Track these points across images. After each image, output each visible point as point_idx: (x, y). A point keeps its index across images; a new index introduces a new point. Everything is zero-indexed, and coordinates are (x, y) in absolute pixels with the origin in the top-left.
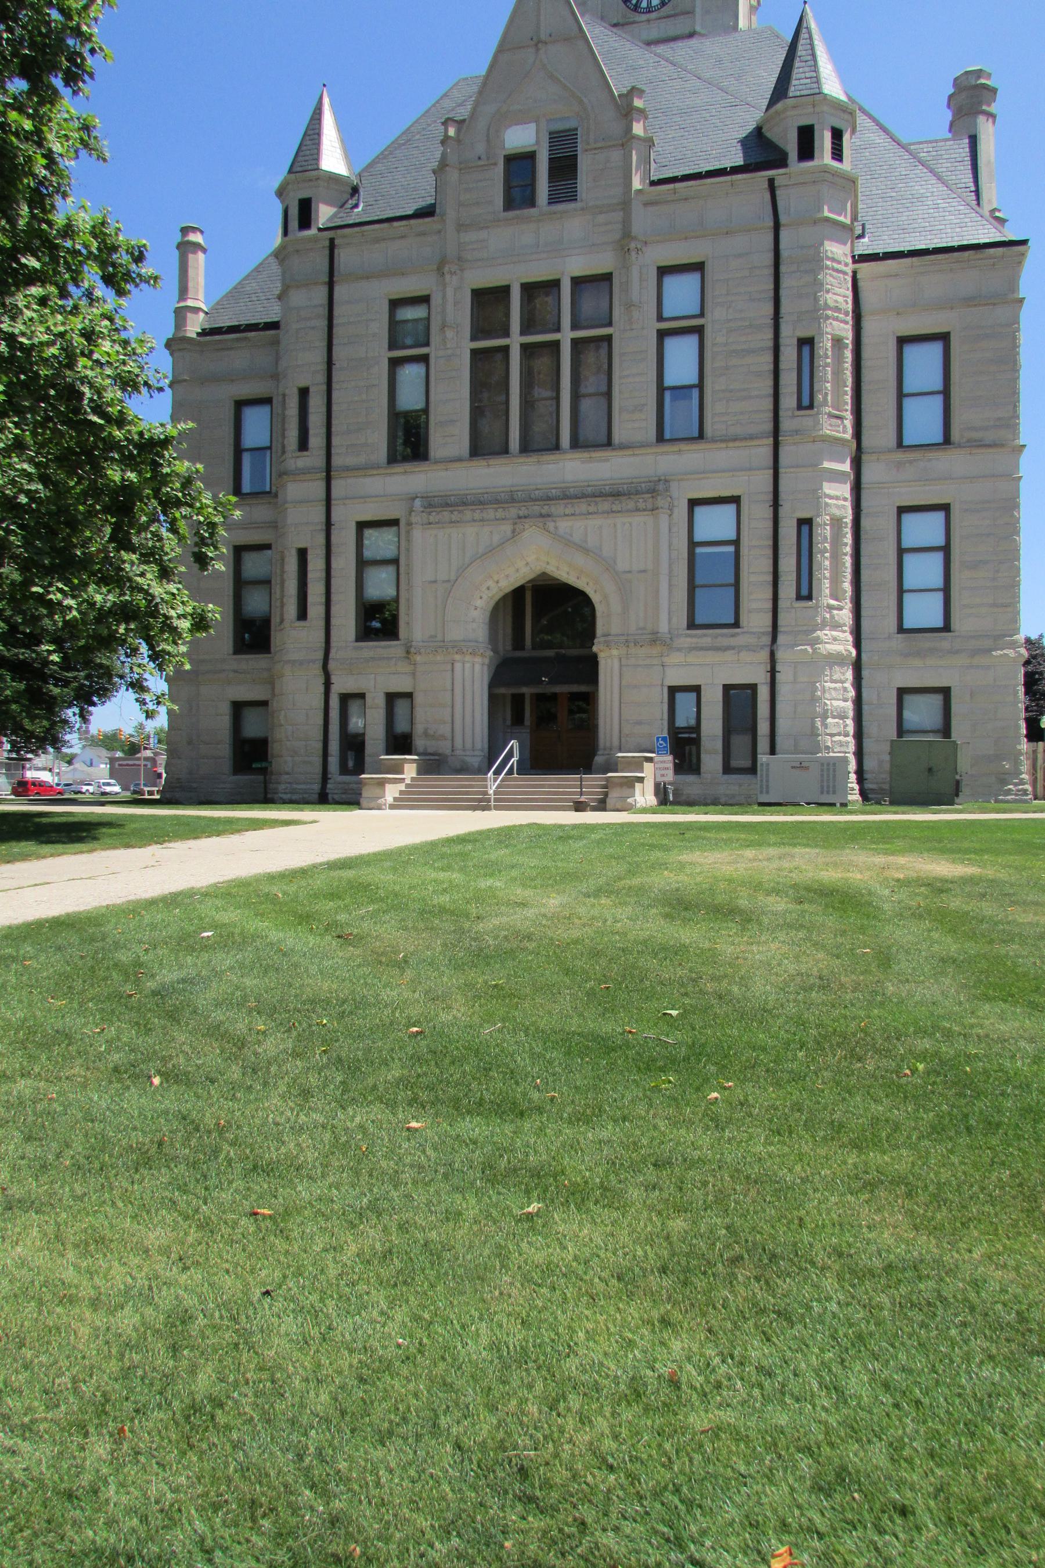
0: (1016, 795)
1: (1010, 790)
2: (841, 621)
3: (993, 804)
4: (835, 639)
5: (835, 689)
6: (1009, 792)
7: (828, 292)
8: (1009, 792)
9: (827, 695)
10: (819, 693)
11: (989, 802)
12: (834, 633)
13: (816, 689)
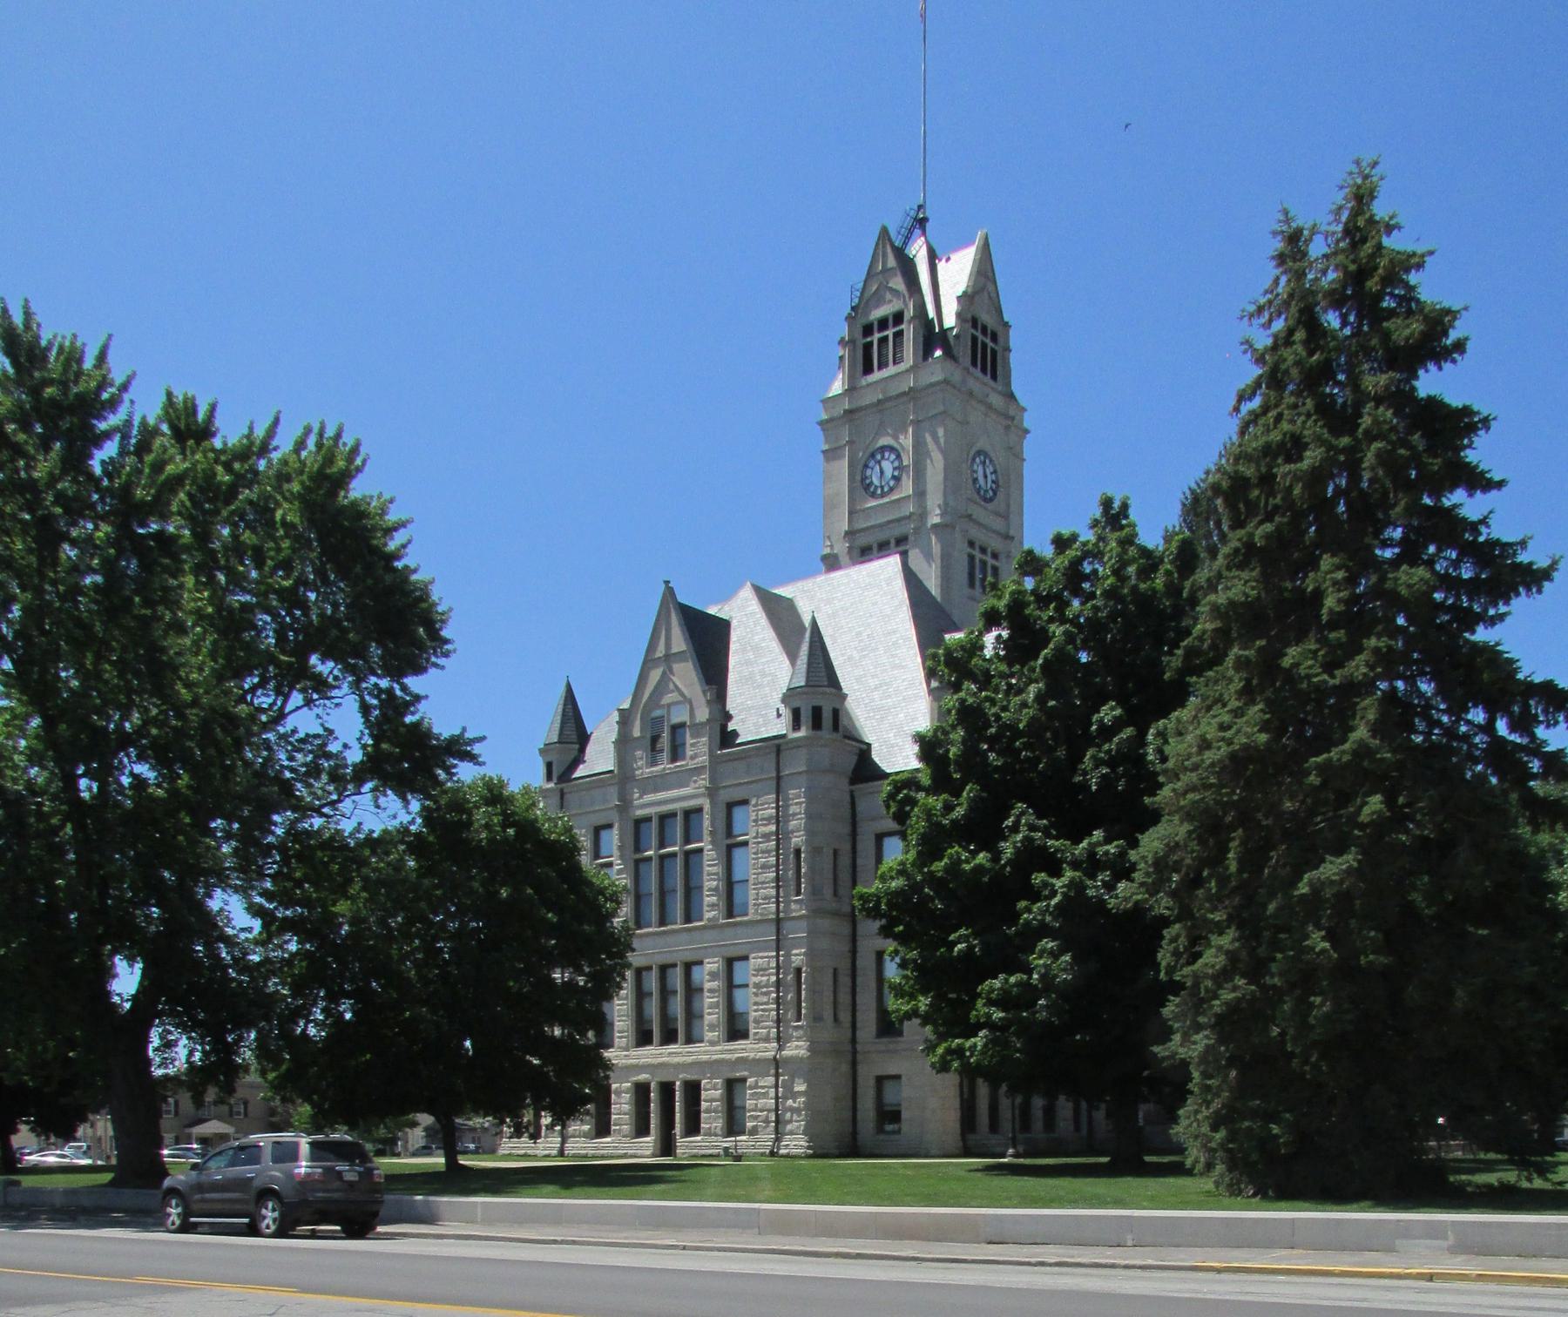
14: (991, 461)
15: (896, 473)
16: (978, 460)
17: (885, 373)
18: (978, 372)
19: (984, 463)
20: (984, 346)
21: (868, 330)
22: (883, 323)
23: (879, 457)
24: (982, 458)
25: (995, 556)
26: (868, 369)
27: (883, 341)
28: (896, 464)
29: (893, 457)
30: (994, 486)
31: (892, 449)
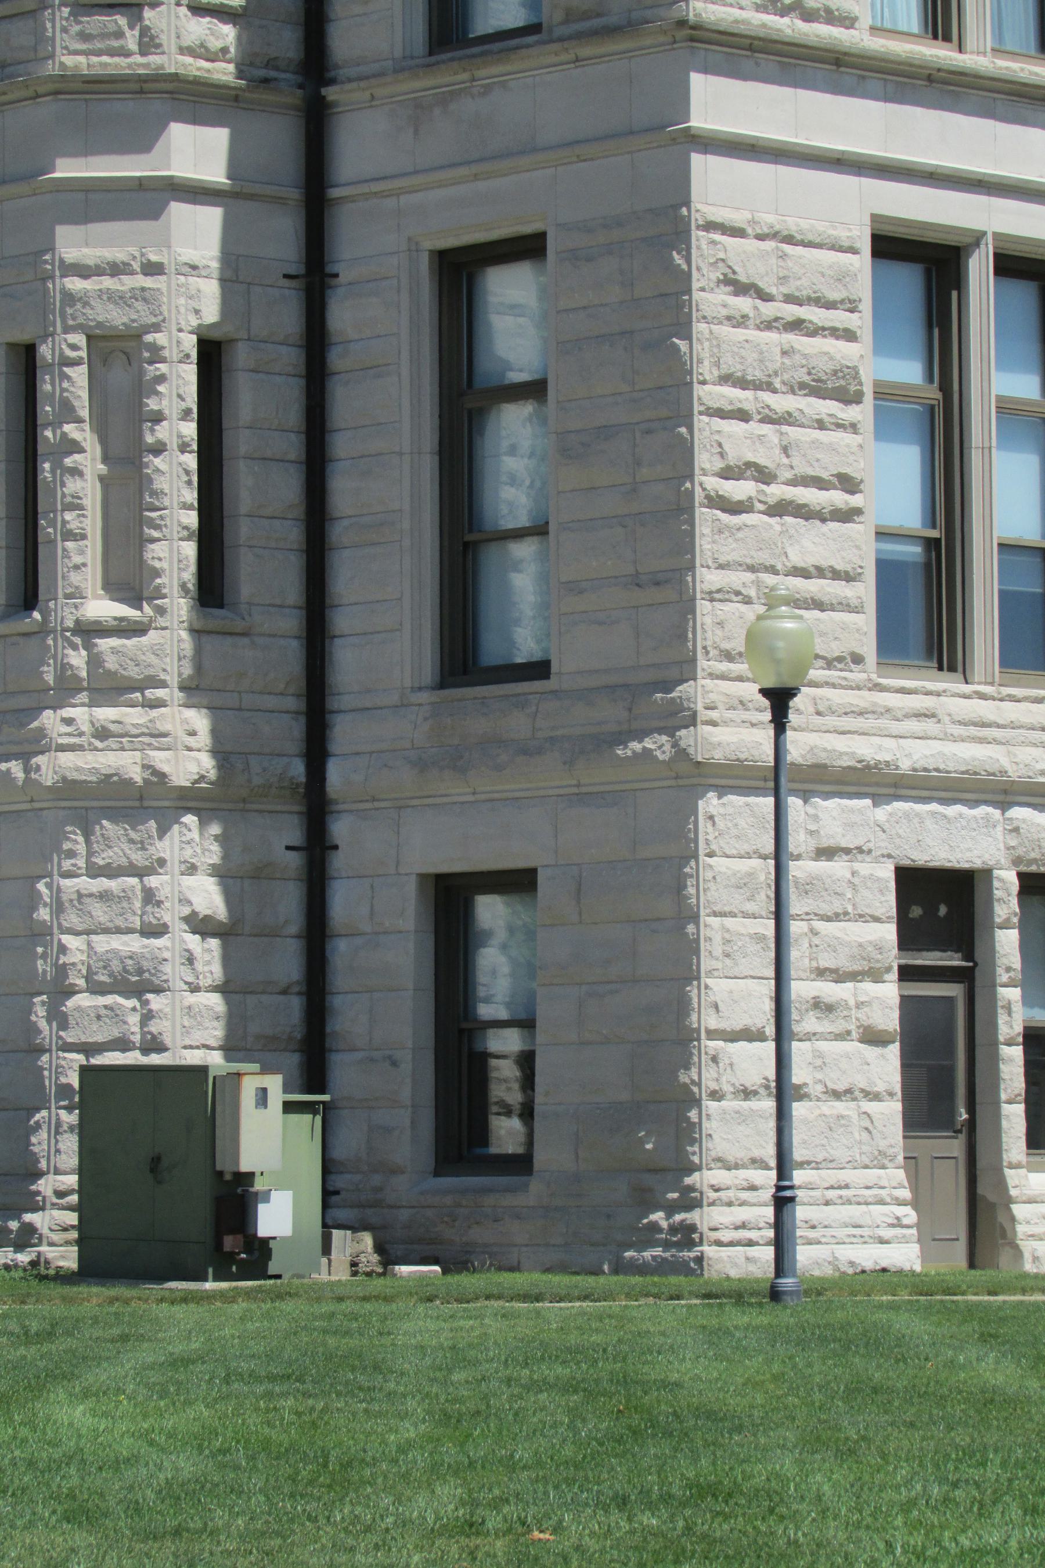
0: (667, 1245)
1: (654, 1227)
2: (134, 672)
3: (606, 1281)
4: (102, 733)
5: (104, 896)
6: (649, 1236)
8: (649, 1236)
9: (72, 919)
10: (43, 914)
11: (597, 1272)
12: (106, 714)
13: (34, 900)
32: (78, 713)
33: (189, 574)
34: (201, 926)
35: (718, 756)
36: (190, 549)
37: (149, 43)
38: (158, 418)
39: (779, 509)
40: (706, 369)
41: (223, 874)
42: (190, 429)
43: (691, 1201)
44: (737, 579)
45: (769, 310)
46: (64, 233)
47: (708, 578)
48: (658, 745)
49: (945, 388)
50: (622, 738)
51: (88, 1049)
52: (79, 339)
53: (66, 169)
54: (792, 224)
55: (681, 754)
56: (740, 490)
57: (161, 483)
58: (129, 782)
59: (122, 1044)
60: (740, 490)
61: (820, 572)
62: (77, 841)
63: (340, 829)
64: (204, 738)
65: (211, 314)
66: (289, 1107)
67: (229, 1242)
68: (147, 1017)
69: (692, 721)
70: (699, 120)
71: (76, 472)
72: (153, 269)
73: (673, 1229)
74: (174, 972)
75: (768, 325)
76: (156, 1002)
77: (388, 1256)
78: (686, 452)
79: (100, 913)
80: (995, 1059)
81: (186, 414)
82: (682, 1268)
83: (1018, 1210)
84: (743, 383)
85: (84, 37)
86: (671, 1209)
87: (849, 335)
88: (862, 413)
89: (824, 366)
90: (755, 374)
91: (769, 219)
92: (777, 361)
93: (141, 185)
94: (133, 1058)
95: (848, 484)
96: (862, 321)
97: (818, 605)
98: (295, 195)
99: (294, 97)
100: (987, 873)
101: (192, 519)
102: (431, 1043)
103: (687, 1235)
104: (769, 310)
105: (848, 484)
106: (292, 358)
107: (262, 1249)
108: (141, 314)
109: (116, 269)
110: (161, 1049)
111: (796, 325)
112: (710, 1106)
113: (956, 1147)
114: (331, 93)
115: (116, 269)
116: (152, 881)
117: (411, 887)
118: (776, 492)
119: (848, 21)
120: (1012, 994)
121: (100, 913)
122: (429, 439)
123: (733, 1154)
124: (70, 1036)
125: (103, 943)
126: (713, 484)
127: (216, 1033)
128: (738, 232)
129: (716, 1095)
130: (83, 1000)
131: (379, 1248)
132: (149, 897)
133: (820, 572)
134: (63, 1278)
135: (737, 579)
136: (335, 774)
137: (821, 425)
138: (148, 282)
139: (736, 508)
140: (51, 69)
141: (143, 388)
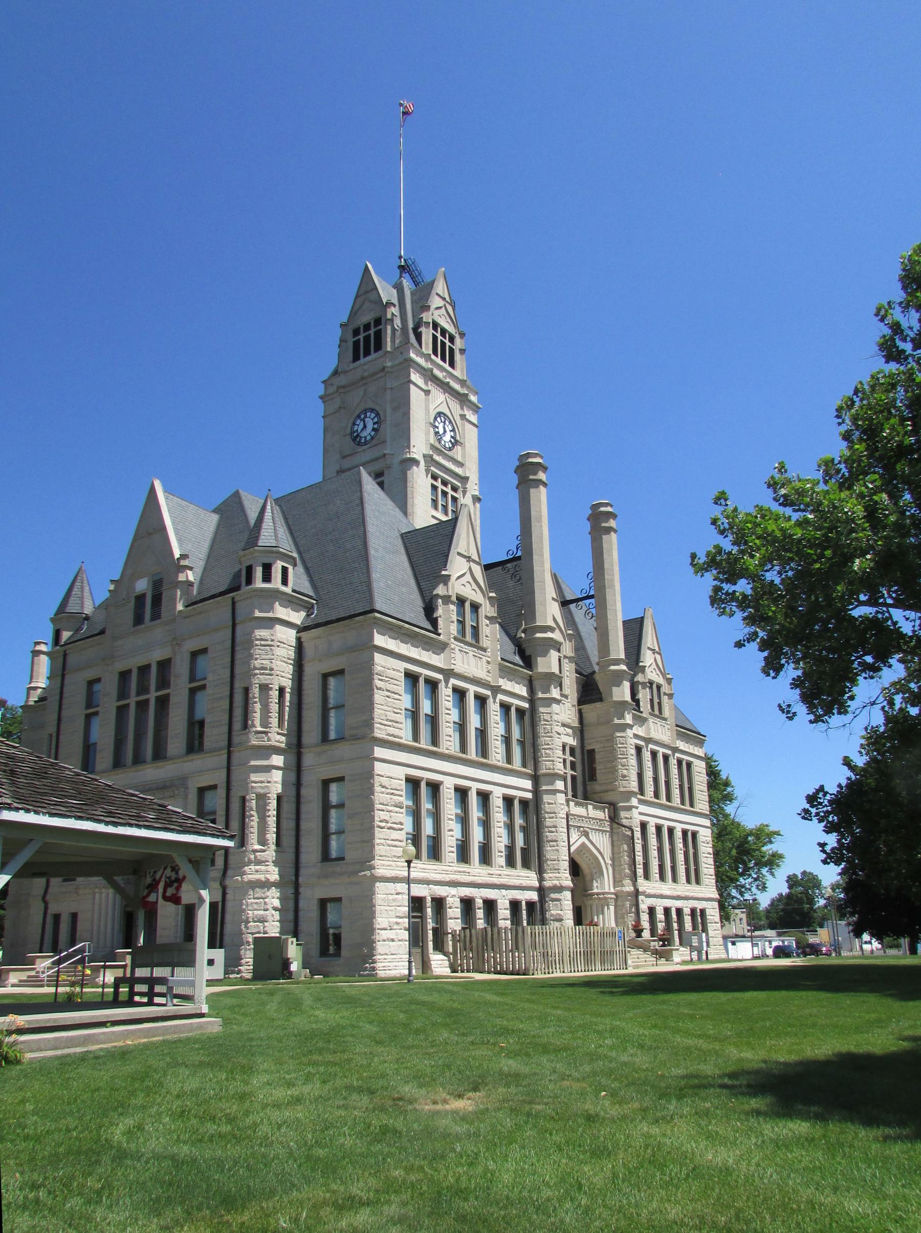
1: (367, 967)
2: (263, 859)
3: (357, 978)
4: (257, 871)
5: (256, 903)
6: (366, 969)
7: (256, 659)
8: (366, 969)
9: (250, 908)
10: (244, 907)
12: (257, 867)
14: (450, 422)
15: (376, 426)
16: (439, 419)
17: (369, 358)
18: (438, 360)
19: (445, 423)
20: (443, 344)
21: (356, 332)
22: (367, 327)
23: (363, 416)
24: (442, 418)
25: (455, 489)
26: (356, 358)
27: (367, 339)
28: (376, 420)
29: (373, 415)
30: (453, 440)
31: (372, 410)
32: (252, 867)
33: (275, 841)
34: (275, 909)
35: (379, 875)
36: (275, 836)
37: (269, 740)
38: (269, 810)
39: (390, 828)
40: (377, 802)
41: (280, 899)
42: (275, 813)
43: (374, 962)
44: (382, 841)
45: (388, 791)
46: (252, 775)
47: (377, 841)
48: (368, 873)
49: (417, 806)
50: (361, 872)
51: (252, 934)
52: (254, 795)
53: (253, 763)
54: (392, 775)
55: (372, 875)
56: (383, 824)
57: (269, 823)
58: (261, 881)
59: (259, 933)
60: (383, 824)
61: (396, 840)
62: (251, 893)
63: (301, 890)
64: (277, 872)
65: (280, 791)
66: (297, 945)
67: (285, 972)
68: (264, 927)
69: (374, 868)
70: (376, 755)
71: (252, 820)
72: (269, 782)
73: (371, 968)
74: (270, 918)
75: (387, 794)
76: (266, 924)
77: (313, 974)
78: (373, 817)
79: (255, 906)
80: (427, 933)
81: (274, 810)
82: (373, 975)
83: (432, 962)
84: (383, 804)
85: (257, 738)
86: (370, 964)
87: (401, 796)
88: (403, 810)
89: (397, 801)
90: (385, 803)
91: (388, 774)
92: (389, 800)
93: (267, 766)
94: (261, 935)
95: (401, 824)
96: (403, 793)
97: (396, 846)
98: (295, 769)
99: (296, 751)
100: (425, 898)
101: (275, 830)
102: (319, 931)
103: (374, 969)
104: (388, 791)
105: (401, 824)
106: (294, 799)
107: (291, 973)
108: (266, 790)
109: (262, 782)
110: (267, 933)
111: (392, 794)
112: (378, 943)
113: (420, 950)
114: (302, 750)
115: (262, 782)
116: (266, 900)
117: (316, 902)
118: (389, 825)
119: (401, 738)
120: (430, 921)
121: (255, 906)
122: (320, 815)
123: (382, 953)
124: (249, 931)
125: (256, 912)
126: (378, 823)
127: (278, 930)
128: (383, 776)
129: (379, 941)
130: (252, 924)
131: (310, 972)
132: (265, 903)
133: (396, 840)
134: (248, 980)
135: (382, 841)
136: (301, 879)
137: (397, 813)
138: (268, 785)
139: (382, 828)
140: (250, 744)
141: (266, 804)
